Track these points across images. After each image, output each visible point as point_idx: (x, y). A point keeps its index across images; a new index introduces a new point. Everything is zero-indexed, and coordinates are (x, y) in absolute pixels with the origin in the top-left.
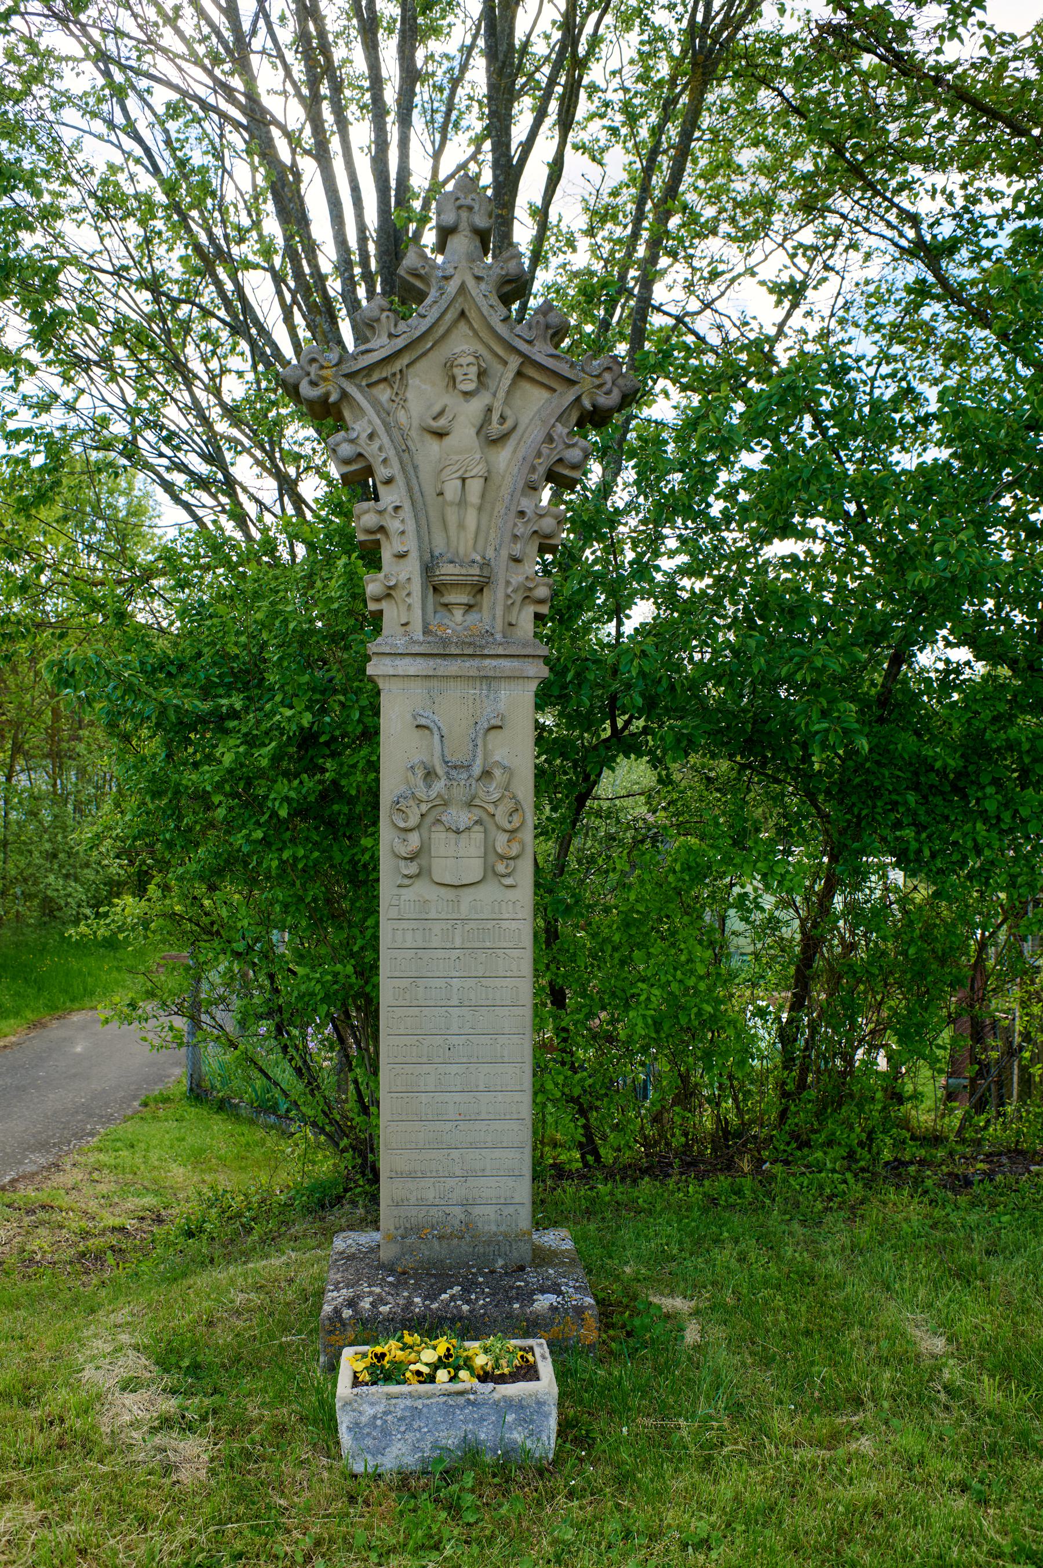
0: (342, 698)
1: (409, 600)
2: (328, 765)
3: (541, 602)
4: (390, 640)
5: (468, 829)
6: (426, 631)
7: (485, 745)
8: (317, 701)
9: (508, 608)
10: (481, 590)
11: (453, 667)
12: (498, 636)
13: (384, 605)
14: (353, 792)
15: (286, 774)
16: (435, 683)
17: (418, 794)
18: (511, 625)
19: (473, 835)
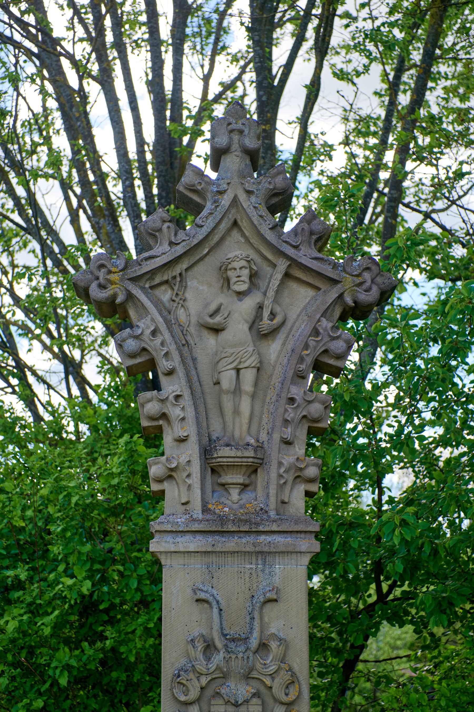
0: (121, 568)
1: (189, 481)
2: (107, 634)
3: (311, 481)
4: (171, 518)
5: (247, 701)
6: (205, 510)
7: (261, 618)
8: (98, 571)
9: (281, 487)
10: (255, 471)
11: (231, 544)
12: (272, 514)
13: (166, 486)
14: (132, 659)
15: (67, 642)
16: (213, 558)
17: (198, 667)
18: (283, 502)
19: (251, 708)
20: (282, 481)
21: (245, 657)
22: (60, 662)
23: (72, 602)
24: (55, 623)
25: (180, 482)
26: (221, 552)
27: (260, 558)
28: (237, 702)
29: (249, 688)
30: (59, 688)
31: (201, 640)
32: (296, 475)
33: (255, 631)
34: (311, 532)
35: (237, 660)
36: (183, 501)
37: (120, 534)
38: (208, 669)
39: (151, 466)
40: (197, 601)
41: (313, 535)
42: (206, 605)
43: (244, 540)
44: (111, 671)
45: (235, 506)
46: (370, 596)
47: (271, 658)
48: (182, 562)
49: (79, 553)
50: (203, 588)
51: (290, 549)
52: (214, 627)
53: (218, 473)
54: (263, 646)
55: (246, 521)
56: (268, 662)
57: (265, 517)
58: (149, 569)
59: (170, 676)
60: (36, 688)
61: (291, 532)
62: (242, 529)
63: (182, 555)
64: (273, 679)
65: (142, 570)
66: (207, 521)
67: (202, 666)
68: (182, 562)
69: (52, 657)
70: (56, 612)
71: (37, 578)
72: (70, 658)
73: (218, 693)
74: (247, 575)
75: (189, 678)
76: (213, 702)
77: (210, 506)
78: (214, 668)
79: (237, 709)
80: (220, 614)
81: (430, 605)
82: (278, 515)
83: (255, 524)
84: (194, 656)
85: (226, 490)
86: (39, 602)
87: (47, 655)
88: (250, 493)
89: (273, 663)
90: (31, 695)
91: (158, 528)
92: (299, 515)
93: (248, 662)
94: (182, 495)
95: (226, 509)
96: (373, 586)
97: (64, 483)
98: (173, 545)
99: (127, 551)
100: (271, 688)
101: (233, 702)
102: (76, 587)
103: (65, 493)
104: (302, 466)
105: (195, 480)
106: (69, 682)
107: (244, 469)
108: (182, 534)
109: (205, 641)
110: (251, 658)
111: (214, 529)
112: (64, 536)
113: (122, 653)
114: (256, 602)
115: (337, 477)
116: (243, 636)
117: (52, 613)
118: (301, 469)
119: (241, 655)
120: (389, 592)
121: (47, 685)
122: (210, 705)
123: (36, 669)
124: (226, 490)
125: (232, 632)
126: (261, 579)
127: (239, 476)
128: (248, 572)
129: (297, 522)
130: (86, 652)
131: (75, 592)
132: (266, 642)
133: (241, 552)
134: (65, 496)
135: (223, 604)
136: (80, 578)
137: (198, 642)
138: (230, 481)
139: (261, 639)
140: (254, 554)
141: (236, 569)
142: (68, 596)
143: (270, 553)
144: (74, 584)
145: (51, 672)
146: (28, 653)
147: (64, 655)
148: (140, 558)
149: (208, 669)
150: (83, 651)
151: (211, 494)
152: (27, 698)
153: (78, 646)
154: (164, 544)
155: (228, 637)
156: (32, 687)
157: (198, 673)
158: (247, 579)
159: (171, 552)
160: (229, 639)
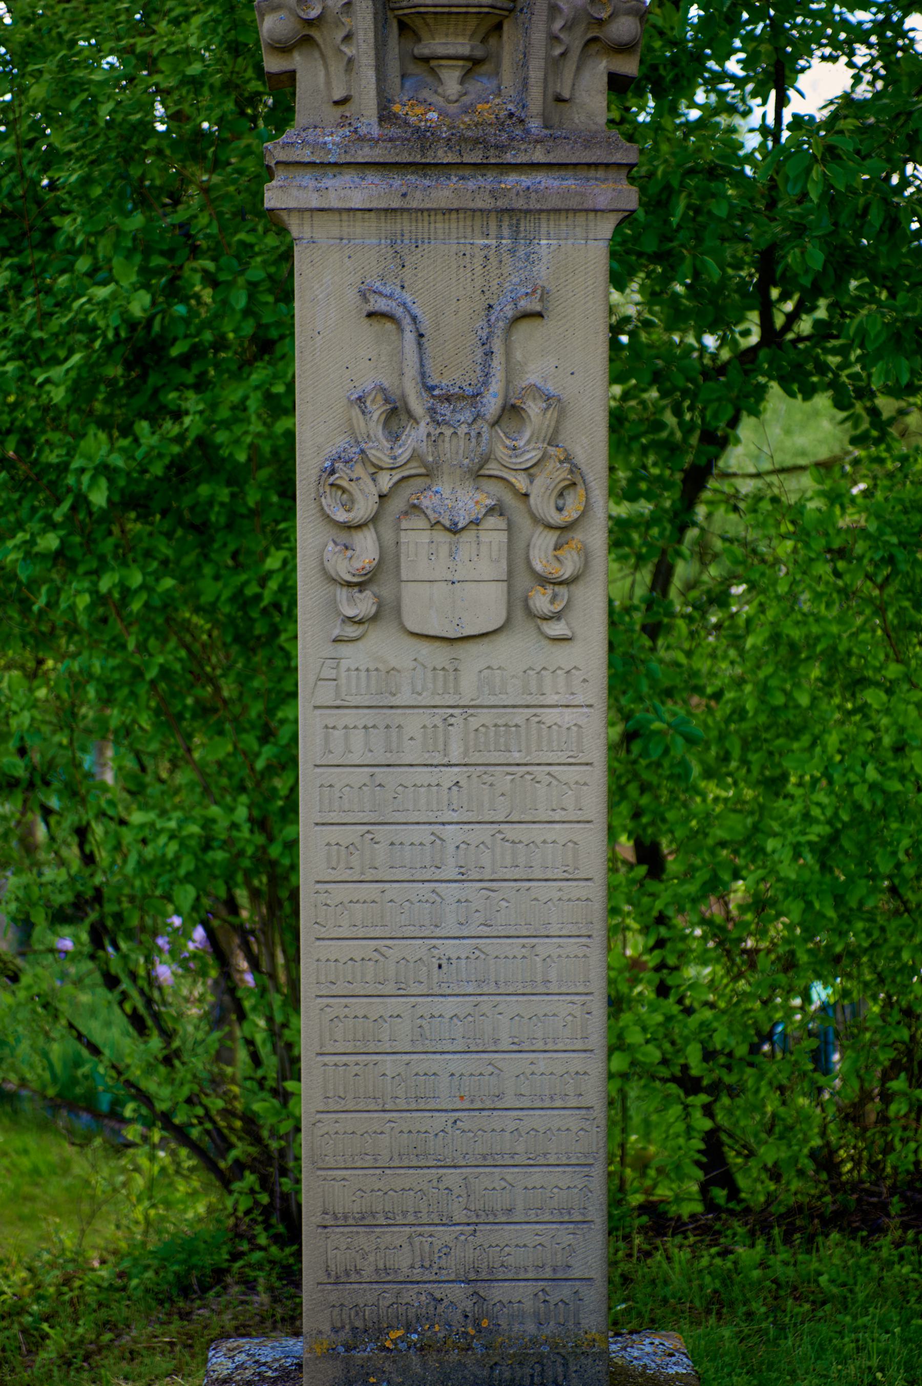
0: (210, 265)
1: (349, 51)
2: (185, 405)
3: (623, 49)
4: (310, 135)
5: (476, 523)
6: (385, 116)
7: (508, 354)
8: (160, 271)
9: (555, 64)
10: (498, 27)
11: (444, 192)
12: (534, 125)
13: (297, 61)
14: (242, 457)
15: (104, 423)
16: (404, 224)
17: (373, 454)
18: (559, 99)
19: (485, 537)
20: (557, 51)
21: (473, 433)
22: (90, 458)
23: (110, 335)
24: (76, 382)
25: (329, 53)
26: (422, 211)
27: (505, 224)
28: (456, 524)
29: (479, 496)
30: (90, 514)
31: (380, 398)
32: (590, 35)
33: (494, 380)
34: (619, 165)
35: (455, 441)
36: (336, 97)
37: (206, 190)
38: (395, 458)
39: (262, 16)
40: (370, 315)
41: (624, 172)
42: (389, 326)
43: (471, 185)
44: (197, 485)
45: (453, 108)
46: (746, 333)
47: (527, 435)
48: (335, 232)
49: (119, 232)
50: (381, 288)
51: (573, 203)
52: (406, 370)
53: (415, 33)
54: (512, 411)
55: (477, 141)
56: (522, 443)
57: (518, 132)
58: (272, 270)
59: (314, 473)
60: (40, 513)
61: (576, 165)
62: (465, 160)
63: (336, 217)
64: (532, 478)
65: (256, 272)
66: (391, 140)
67: (382, 450)
68: (335, 232)
69: (70, 454)
70: (76, 358)
71: (30, 286)
72: (111, 451)
73: (414, 506)
74: (478, 261)
75: (354, 477)
76: (404, 524)
77: (396, 108)
78: (407, 455)
79: (455, 538)
80: (420, 345)
81: (877, 336)
82: (546, 127)
83: (497, 147)
84: (364, 430)
85: (432, 71)
86: (37, 334)
87: (61, 446)
88: (485, 80)
89: (532, 445)
90: (35, 526)
91: (282, 156)
92: (594, 128)
93: (478, 444)
94: (334, 84)
95: (433, 115)
96: (754, 316)
97: (80, 73)
98: (316, 195)
99: (222, 229)
100: (526, 495)
101: (447, 524)
102: (117, 303)
103: (84, 96)
104: (604, 15)
105: (364, 46)
106: (109, 501)
107: (472, 23)
108: (336, 170)
109: (387, 400)
110: (485, 436)
111: (405, 158)
112: (87, 196)
113: (220, 446)
114: (497, 319)
115: (683, 64)
116: (469, 390)
117: (66, 359)
118: (600, 22)
119: (463, 429)
120: (787, 327)
121: (66, 506)
122: (398, 530)
123: (39, 477)
124: (432, 71)
125: (444, 382)
126: (506, 270)
127: (461, 40)
128: (479, 255)
129: (589, 142)
130: (143, 441)
131: (116, 313)
132: (518, 403)
133: (465, 210)
134: (84, 103)
135: (426, 325)
136: (125, 283)
137: (373, 401)
138: (441, 51)
139: (506, 396)
140: (493, 215)
141: (454, 248)
142: (101, 323)
143: (528, 211)
144: (114, 296)
145: (71, 480)
146: (21, 442)
147: (96, 445)
148: (251, 246)
149: (395, 458)
150: (136, 440)
151: (398, 80)
152: (24, 531)
153: (126, 430)
154: (295, 192)
155: (436, 392)
156: (34, 510)
157: (374, 465)
158: (479, 270)
159: (312, 210)
160: (439, 396)
